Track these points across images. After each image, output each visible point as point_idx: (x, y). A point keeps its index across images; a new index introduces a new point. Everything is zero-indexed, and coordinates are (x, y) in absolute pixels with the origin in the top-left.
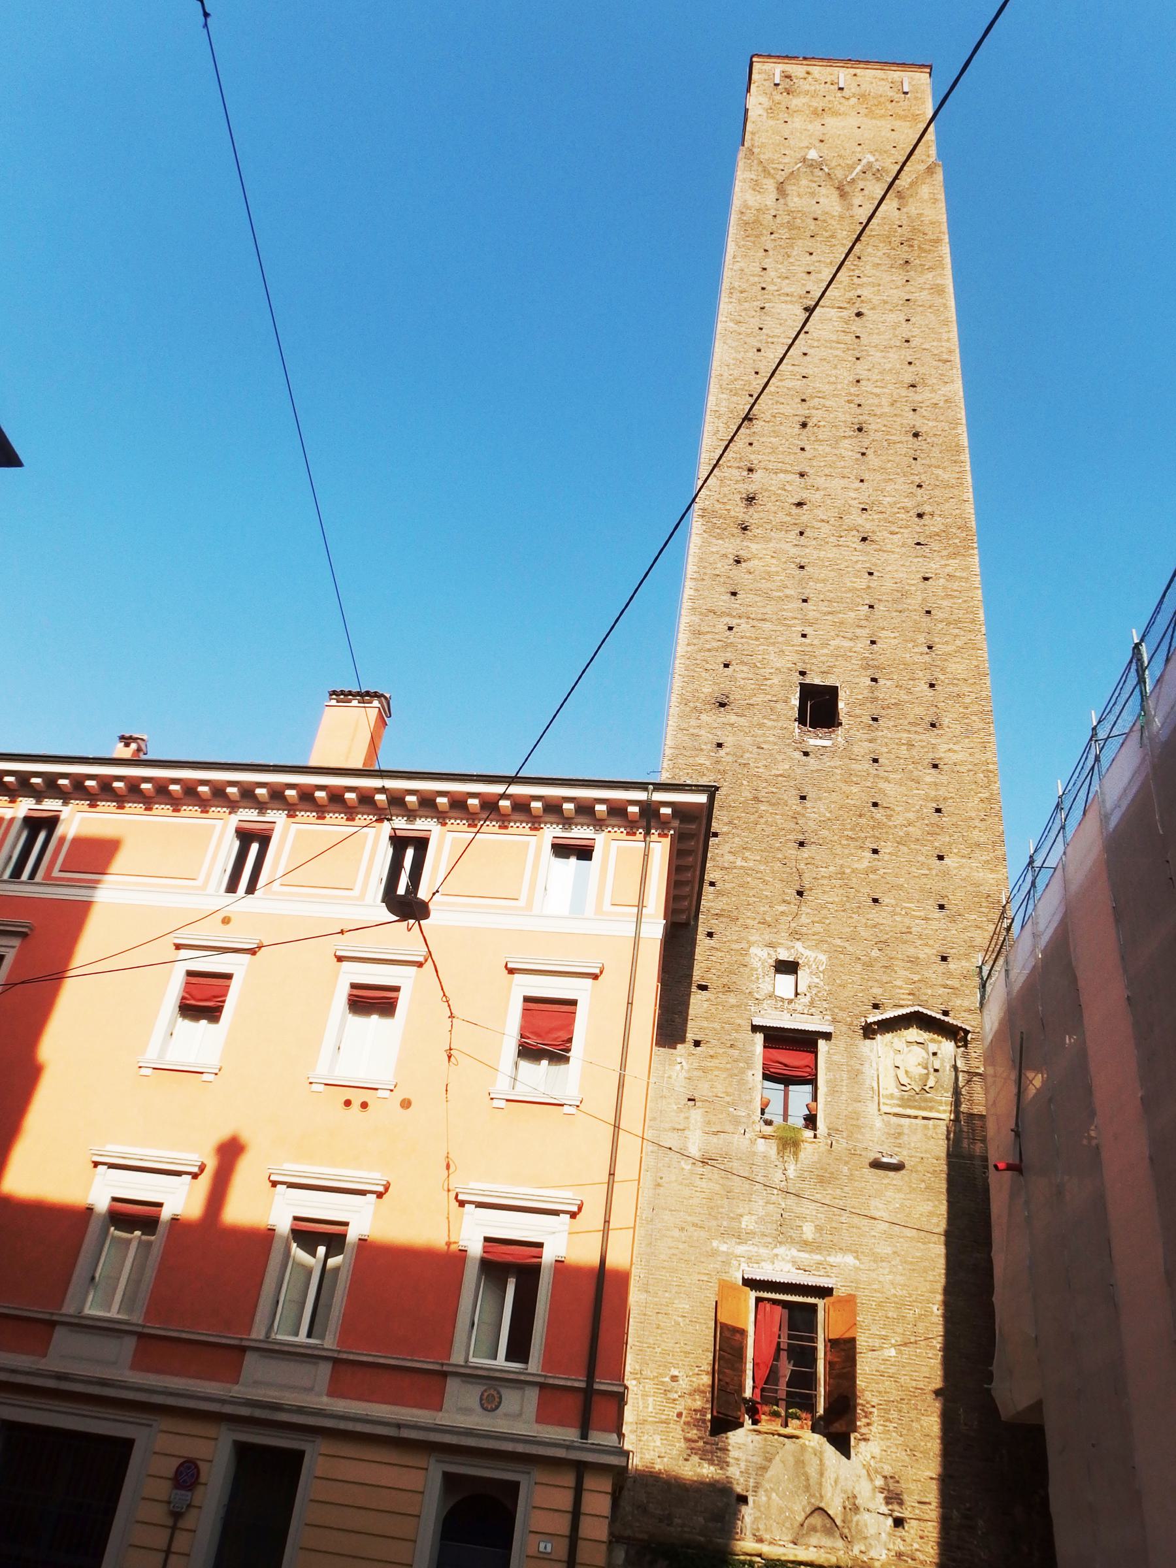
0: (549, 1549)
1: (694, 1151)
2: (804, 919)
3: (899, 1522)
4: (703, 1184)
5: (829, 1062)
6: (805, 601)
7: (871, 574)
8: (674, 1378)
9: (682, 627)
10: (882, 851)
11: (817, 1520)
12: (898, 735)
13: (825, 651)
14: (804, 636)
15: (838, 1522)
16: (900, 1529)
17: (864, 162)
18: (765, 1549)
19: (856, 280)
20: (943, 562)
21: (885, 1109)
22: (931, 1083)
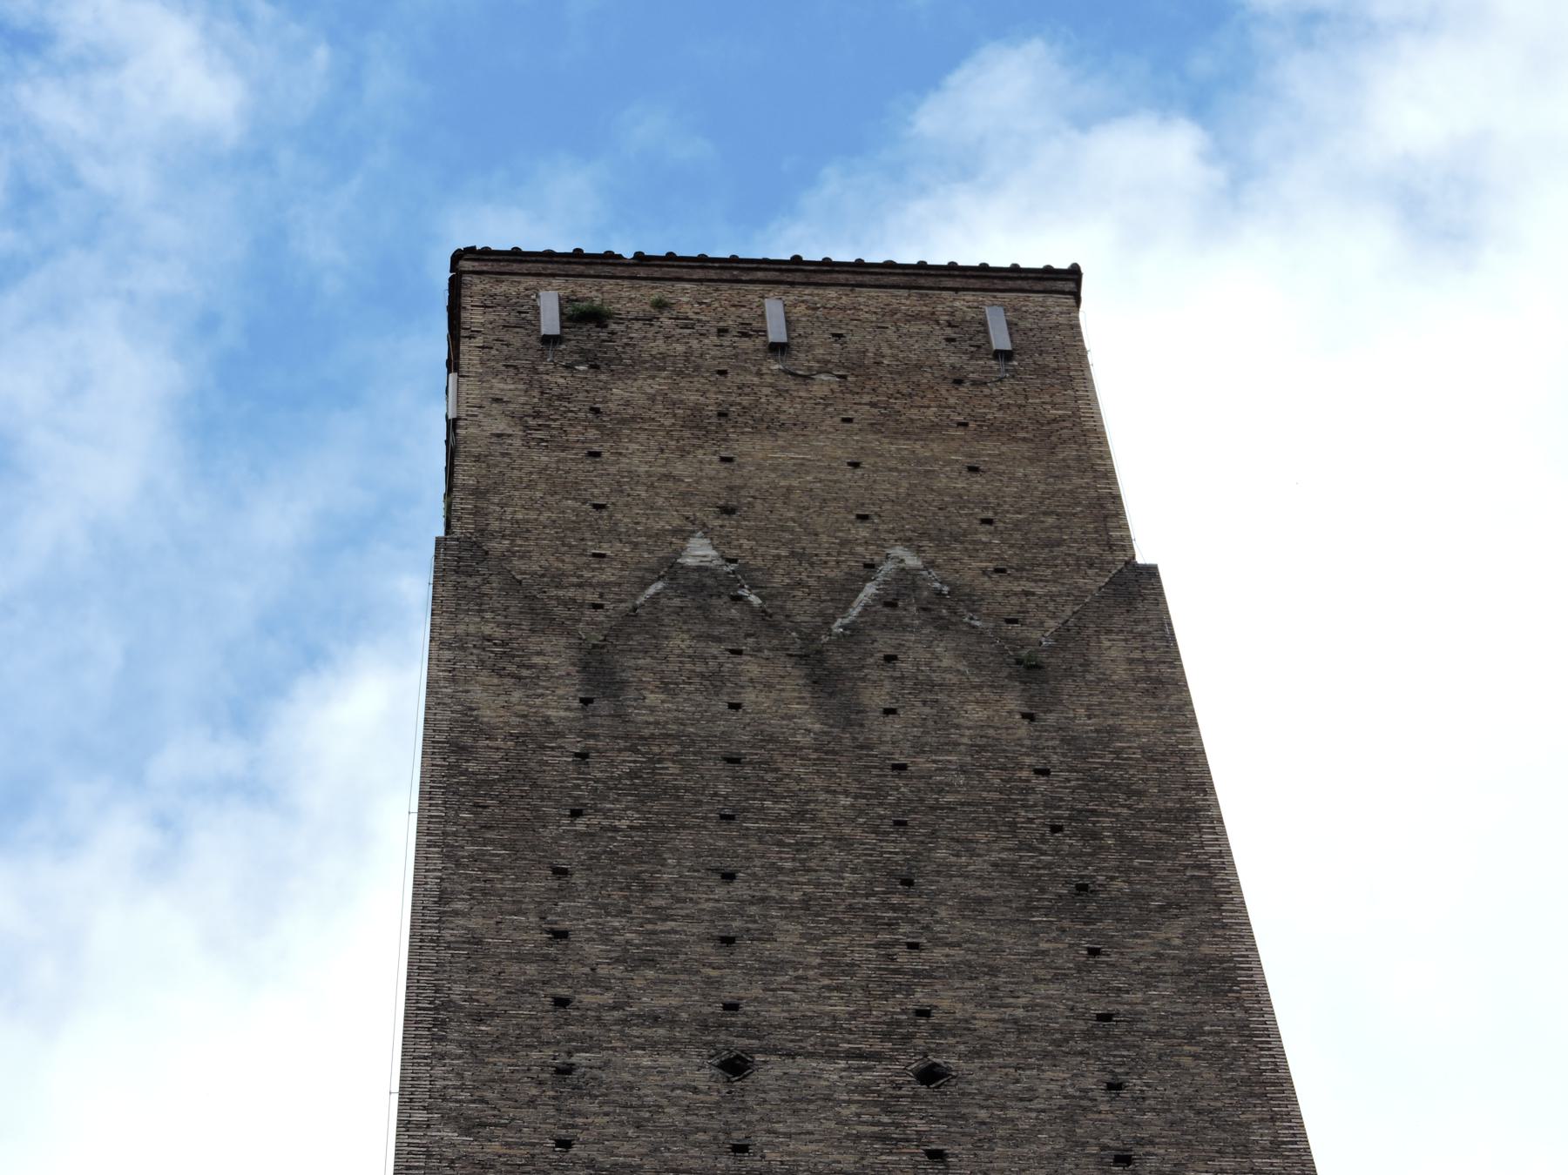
17: (888, 567)
19: (903, 958)
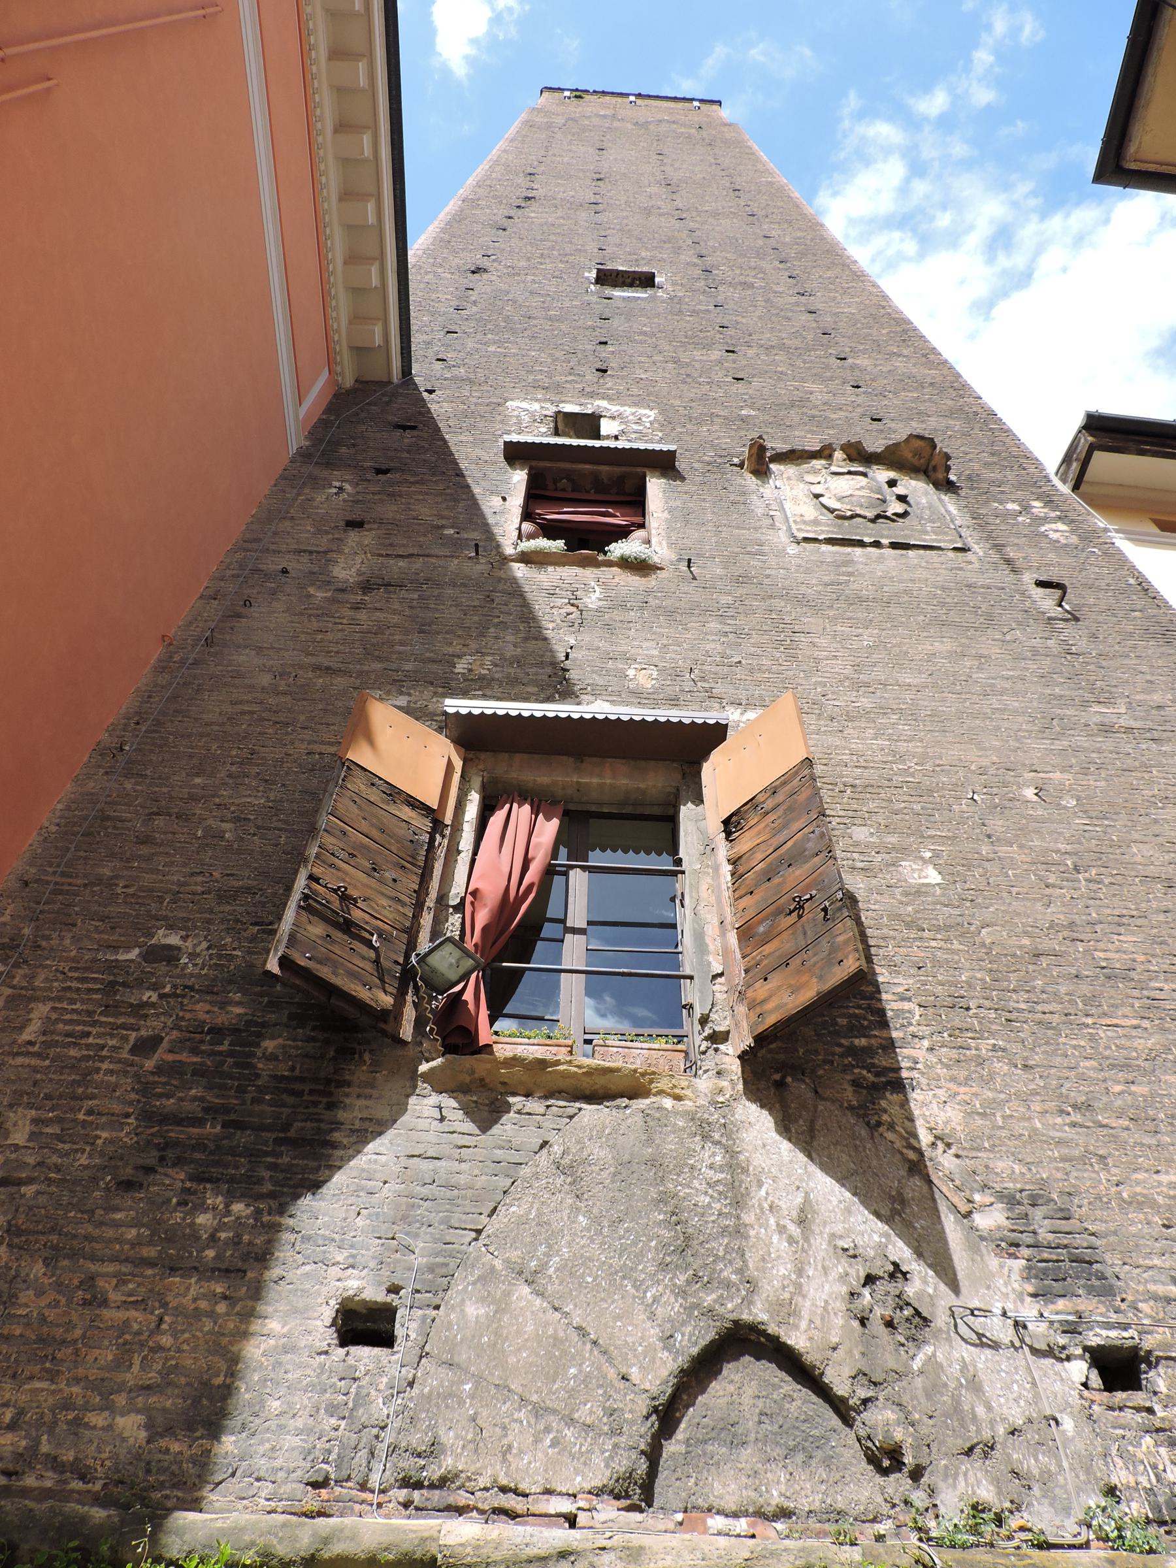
1: (345, 571)
3: (1119, 1369)
4: (362, 615)
15: (839, 1381)
16: (1139, 1398)
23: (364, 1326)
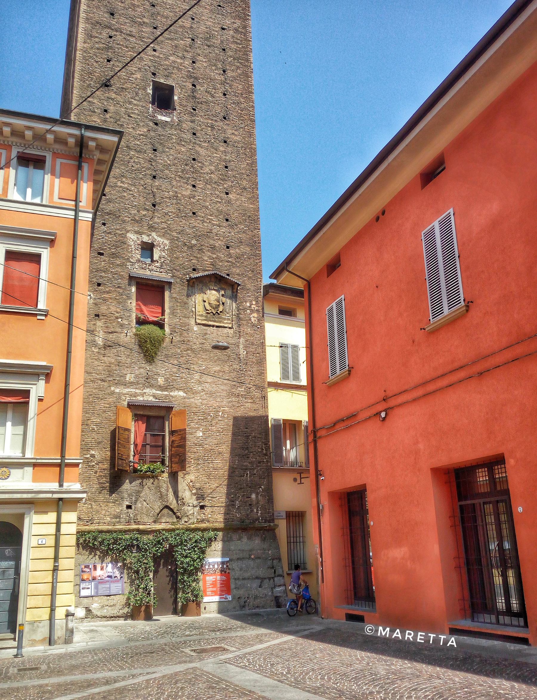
0: (44, 543)
1: (100, 342)
2: (156, 220)
4: (105, 358)
5: (171, 297)
6: (155, 28)
7: (193, 19)
8: (93, 456)
9: (80, 30)
10: (197, 186)
11: (166, 511)
12: (206, 121)
13: (167, 63)
14: (155, 50)
18: (141, 527)
20: (233, 21)
21: (198, 321)
22: (221, 308)
23: (129, 507)
